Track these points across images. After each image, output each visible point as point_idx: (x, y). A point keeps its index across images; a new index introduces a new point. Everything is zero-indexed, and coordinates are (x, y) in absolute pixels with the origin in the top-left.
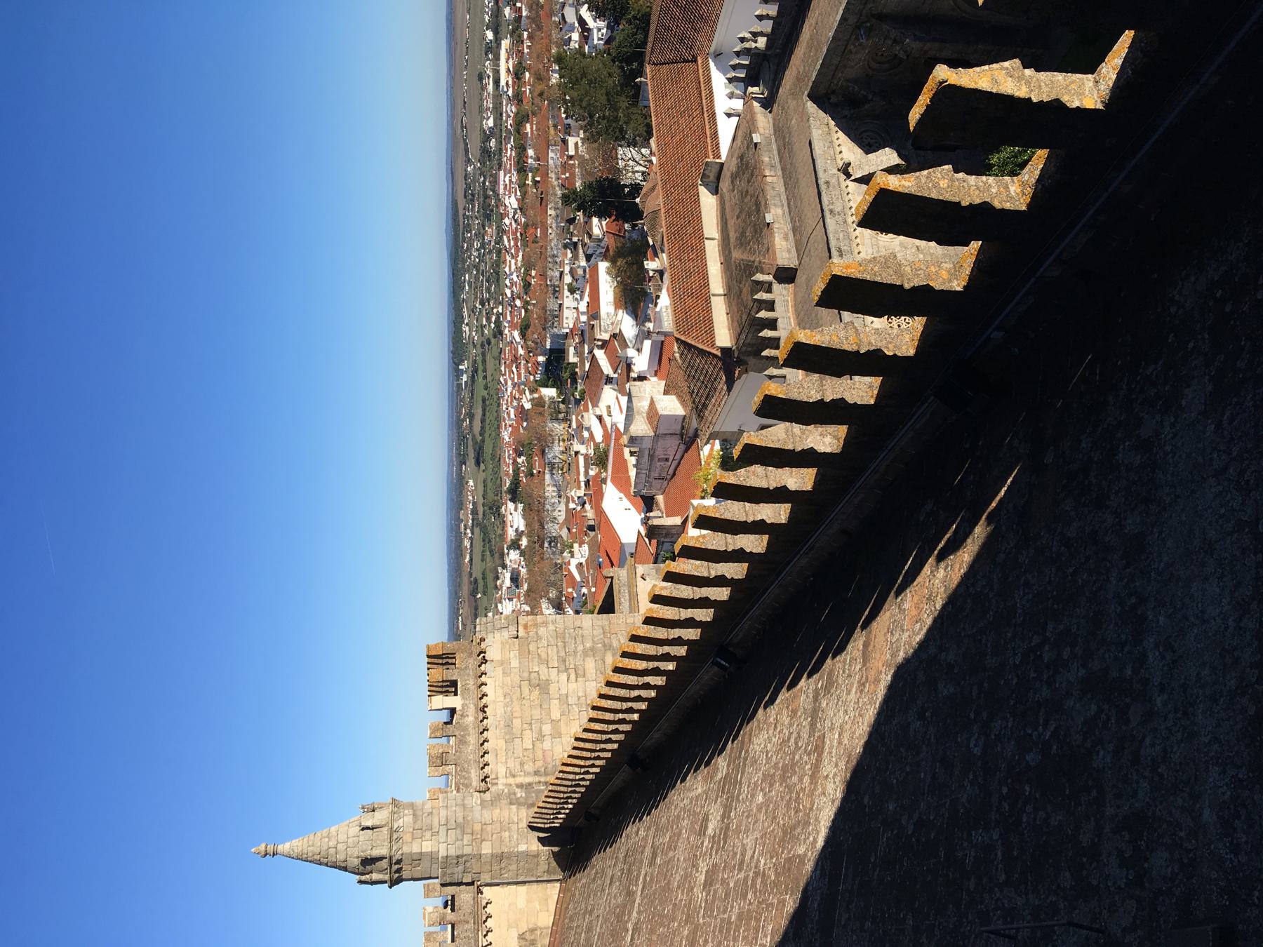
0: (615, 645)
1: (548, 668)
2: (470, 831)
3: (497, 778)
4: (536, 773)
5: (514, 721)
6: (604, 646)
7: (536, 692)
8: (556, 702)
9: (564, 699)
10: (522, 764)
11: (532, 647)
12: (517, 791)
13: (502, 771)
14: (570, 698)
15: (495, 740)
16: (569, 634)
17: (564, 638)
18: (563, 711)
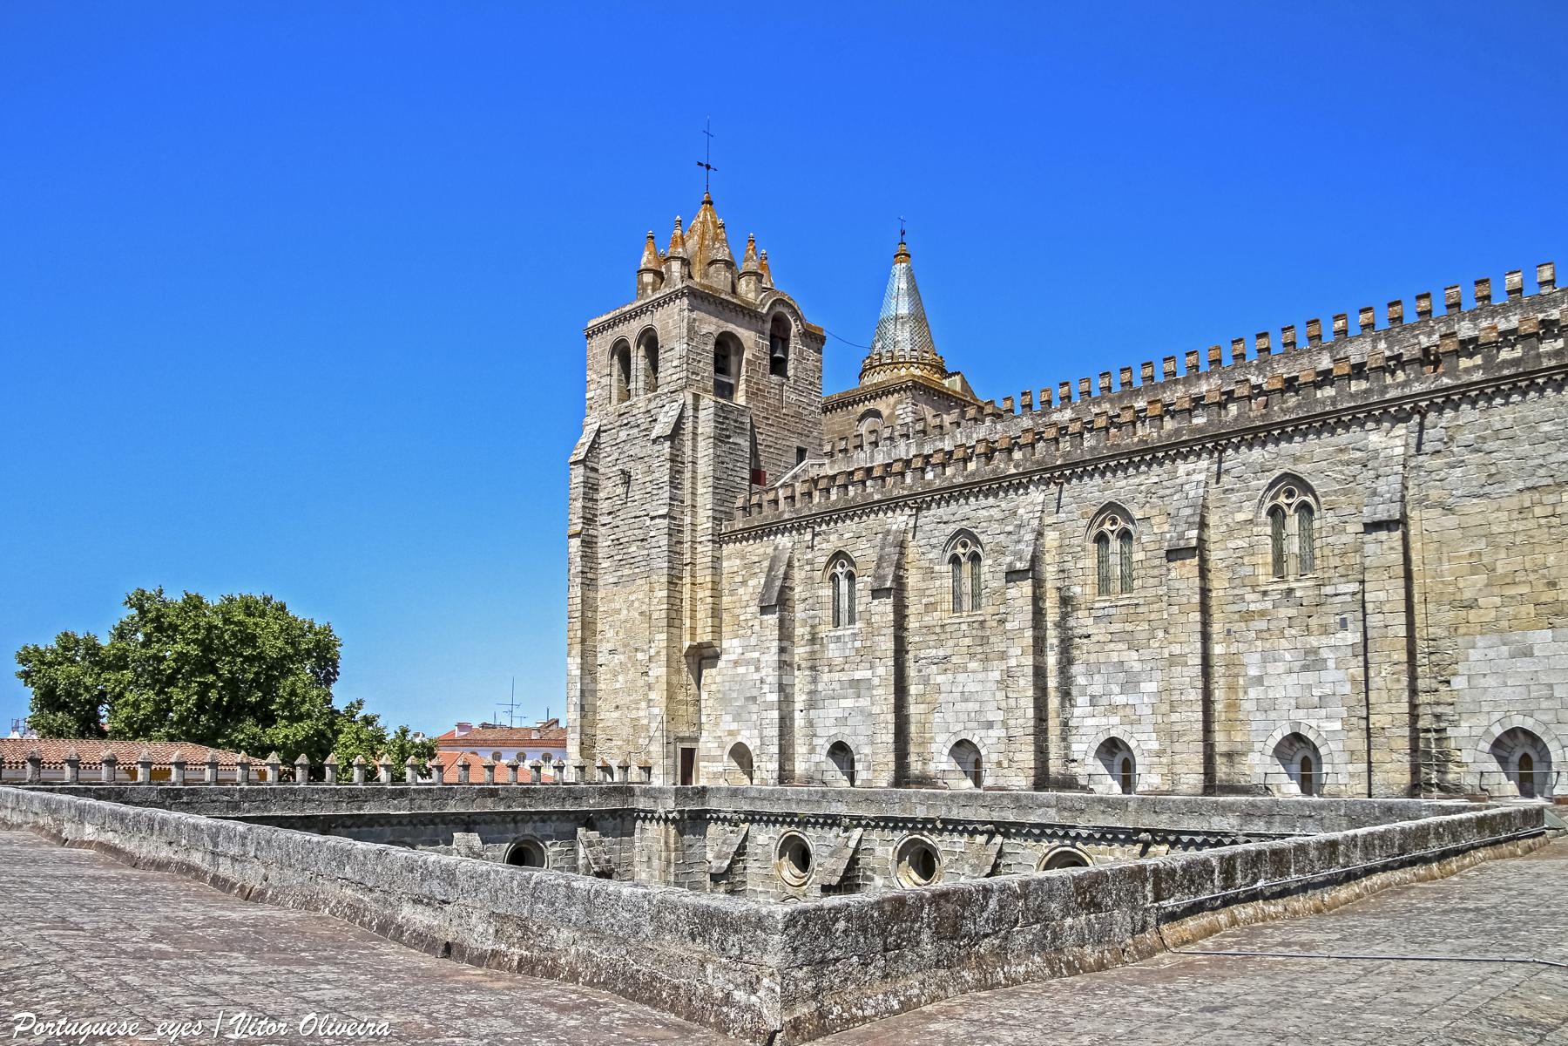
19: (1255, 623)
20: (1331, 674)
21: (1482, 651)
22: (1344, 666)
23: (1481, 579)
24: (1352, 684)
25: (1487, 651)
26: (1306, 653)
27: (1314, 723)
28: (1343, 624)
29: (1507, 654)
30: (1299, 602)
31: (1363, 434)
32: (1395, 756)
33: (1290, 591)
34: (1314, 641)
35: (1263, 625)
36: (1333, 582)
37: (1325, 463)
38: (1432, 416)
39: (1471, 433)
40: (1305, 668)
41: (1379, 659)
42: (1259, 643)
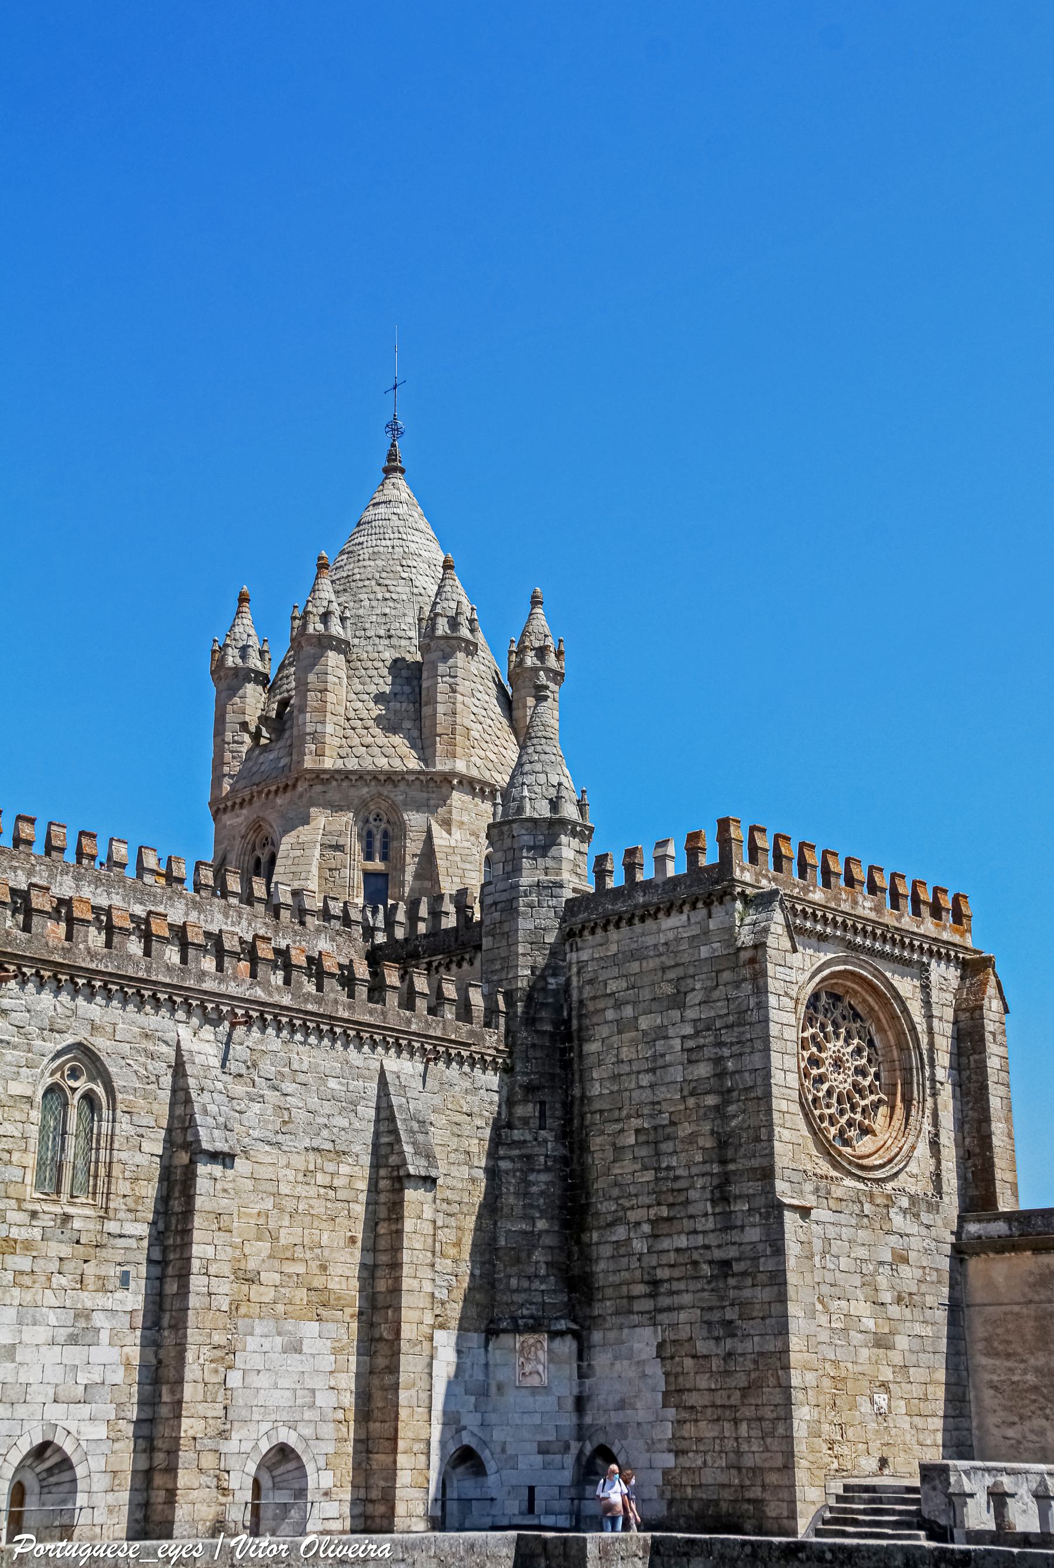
0: (729, 1109)
1: (699, 1004)
2: (503, 918)
3: (577, 950)
4: (581, 1002)
5: (637, 963)
6: (730, 1091)
7: (669, 989)
8: (659, 1021)
9: (660, 1034)
10: (591, 982)
11: (726, 976)
12: (562, 980)
13: (585, 956)
14: (662, 1042)
15: (617, 939)
16: (744, 1033)
17: (739, 1025)
18: (648, 1034)
19: (16, 1259)
20: (104, 1353)
21: (259, 1338)
22: (119, 1343)
23: (265, 1247)
24: (126, 1369)
25: (263, 1339)
26: (76, 1316)
27: (72, 1427)
28: (125, 1280)
29: (279, 1348)
30: (76, 1236)
31: (172, 1023)
32: (204, 1479)
33: (67, 1218)
34: (87, 1299)
35: (23, 1263)
36: (121, 1215)
37: (128, 1046)
38: (240, 1030)
39: (272, 1064)
40: (73, 1340)
41: (200, 1339)
42: (16, 1292)
